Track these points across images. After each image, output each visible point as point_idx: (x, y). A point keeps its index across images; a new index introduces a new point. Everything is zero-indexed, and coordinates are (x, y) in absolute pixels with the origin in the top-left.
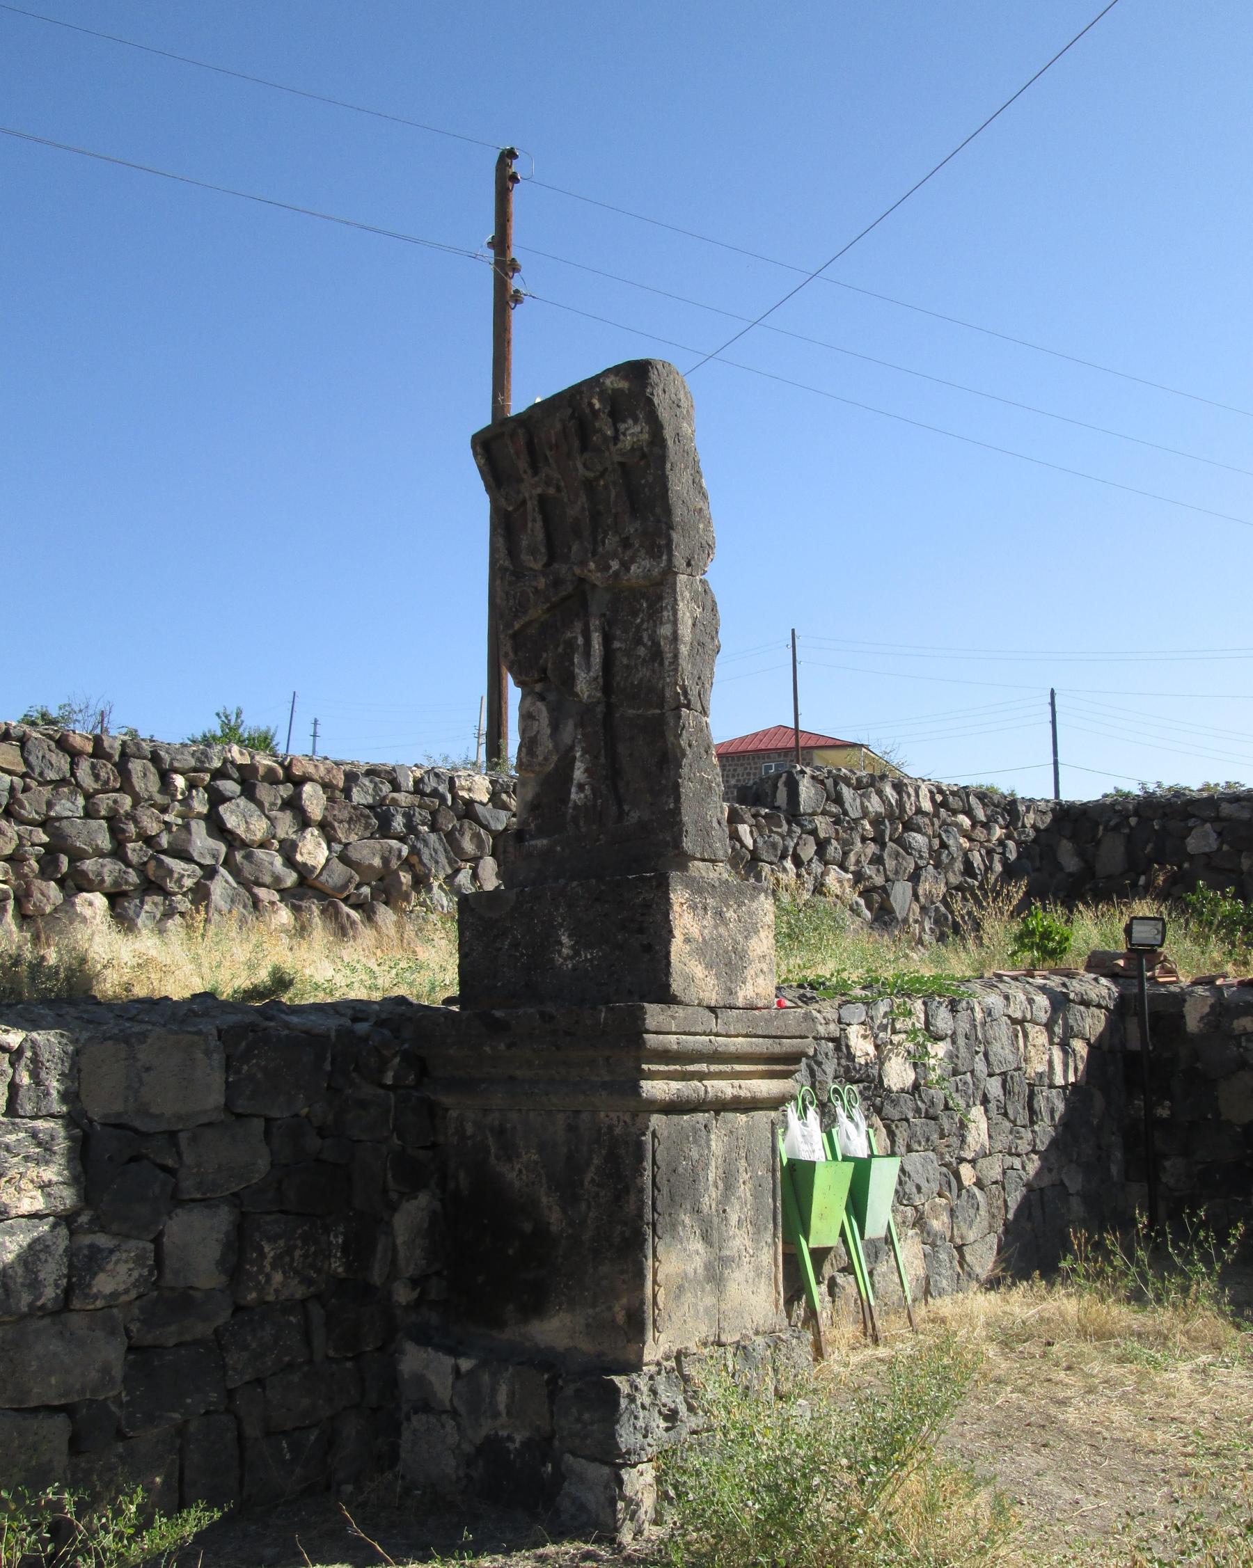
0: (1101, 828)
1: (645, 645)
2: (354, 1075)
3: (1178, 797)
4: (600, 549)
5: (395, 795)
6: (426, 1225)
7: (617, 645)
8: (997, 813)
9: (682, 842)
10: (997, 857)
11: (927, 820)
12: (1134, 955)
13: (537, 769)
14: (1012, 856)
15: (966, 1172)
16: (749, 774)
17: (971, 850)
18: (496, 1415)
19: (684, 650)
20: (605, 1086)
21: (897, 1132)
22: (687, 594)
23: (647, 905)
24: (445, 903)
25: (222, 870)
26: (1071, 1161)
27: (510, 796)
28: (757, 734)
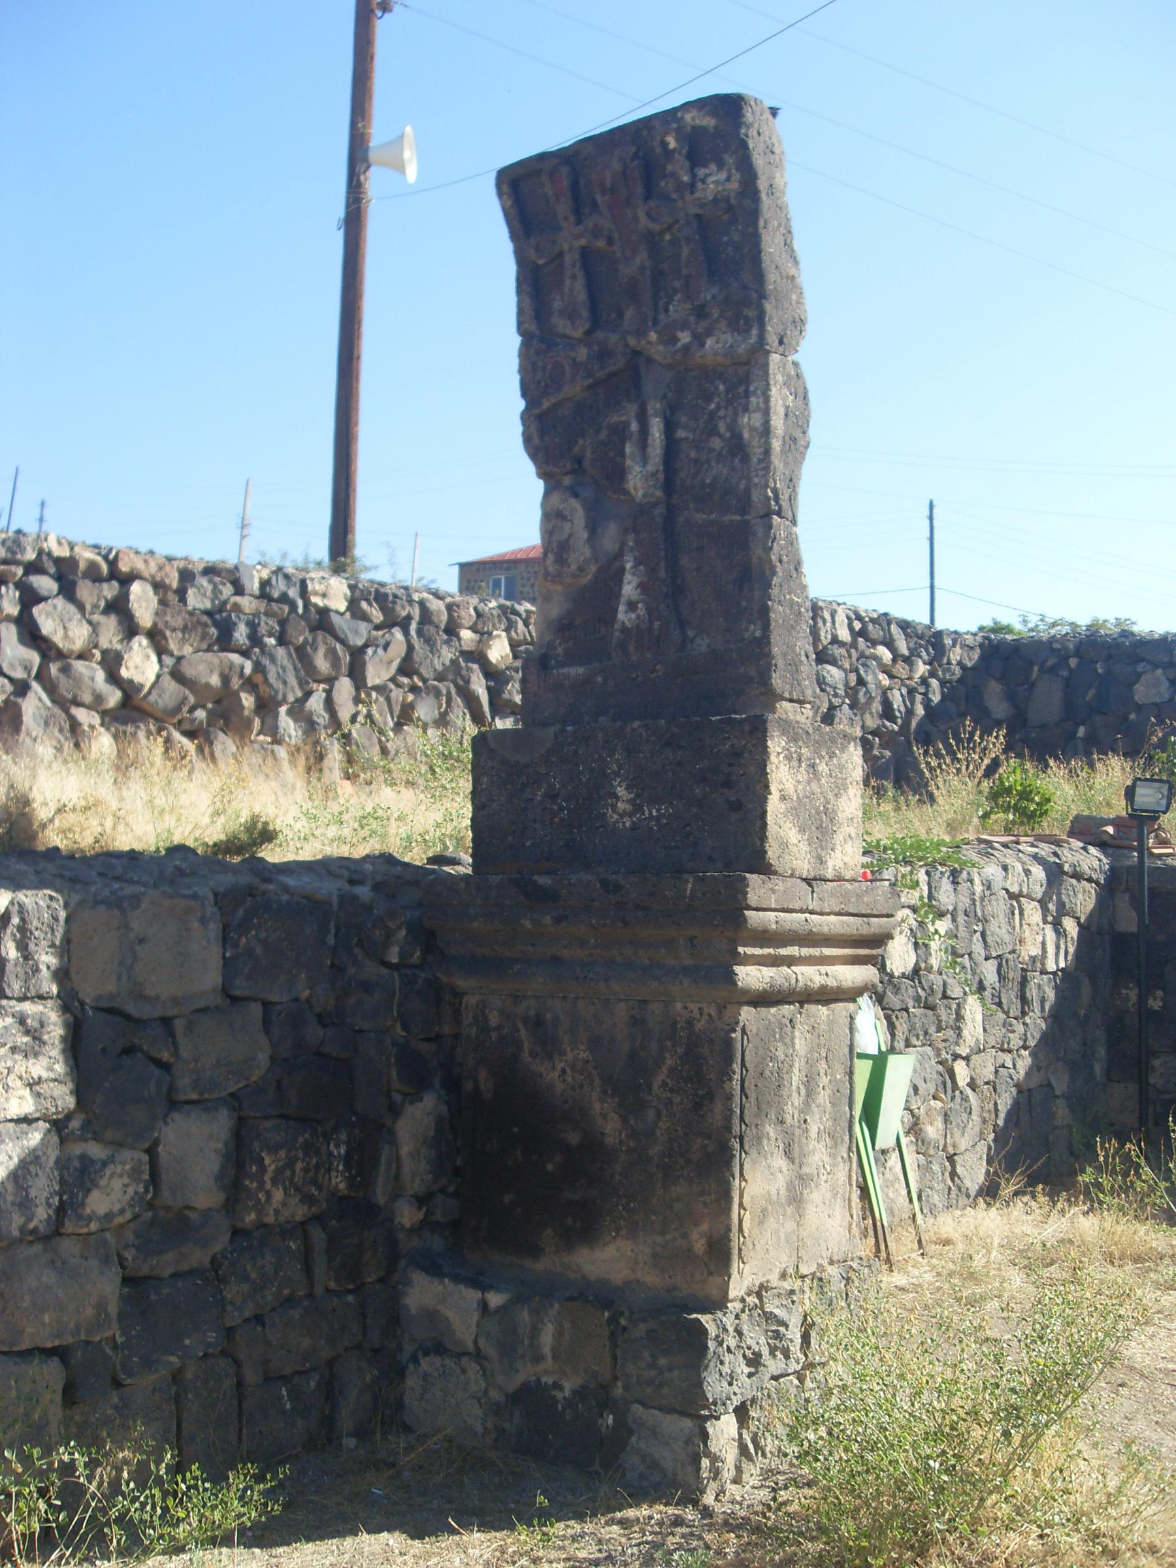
0: (1036, 668)
1: (720, 436)
2: (357, 951)
3: (1126, 637)
4: (662, 317)
5: (238, 599)
6: (432, 1133)
7: (681, 434)
8: (921, 646)
9: (770, 678)
10: (919, 698)
11: (843, 651)
12: (1135, 822)
13: (568, 580)
14: (936, 698)
15: (960, 1068)
17: (890, 688)
18: (538, 1358)
19: (776, 444)
20: (686, 971)
21: (897, 1023)
22: (780, 378)
23: (737, 754)
24: (293, 733)
25: (36, 686)
26: (1058, 1059)
27: (370, 605)
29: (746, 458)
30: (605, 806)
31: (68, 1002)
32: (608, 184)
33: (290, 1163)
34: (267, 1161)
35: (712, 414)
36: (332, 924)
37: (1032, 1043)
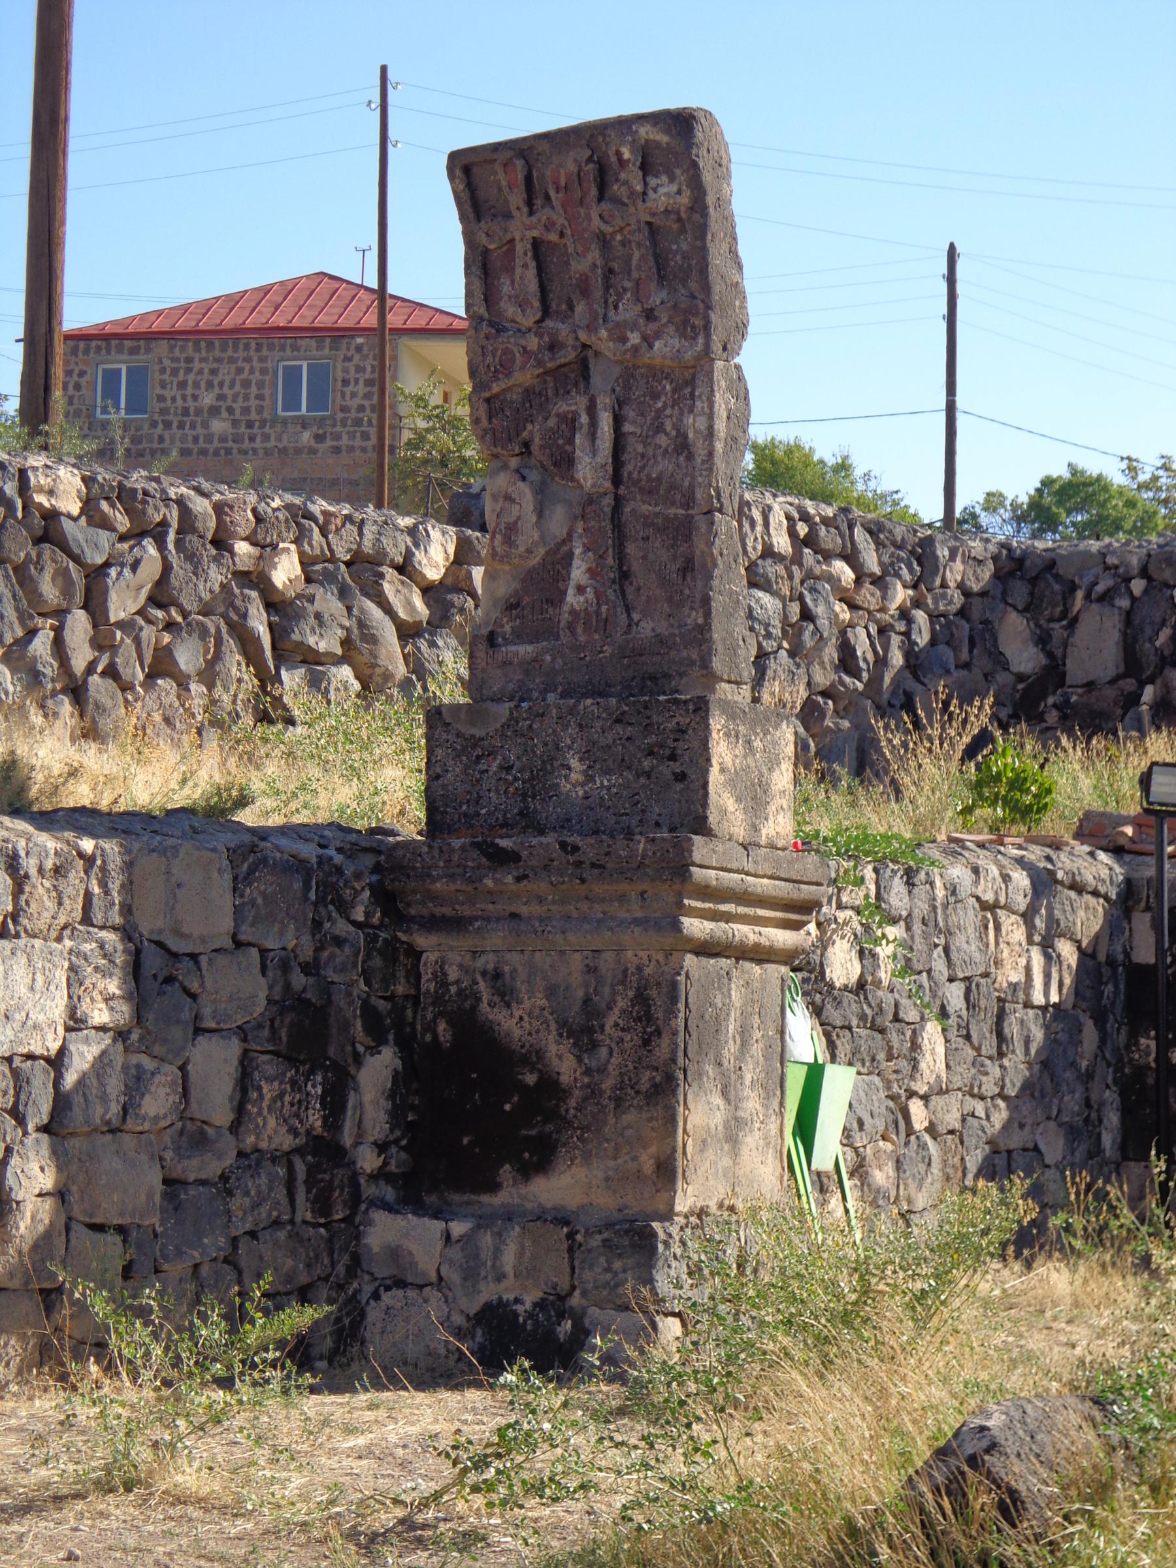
0: (1080, 594)
1: (667, 434)
2: (331, 907)
4: (611, 313)
8: (900, 560)
9: (711, 661)
10: (896, 640)
11: (780, 569)
12: (1152, 820)
13: (516, 561)
14: (922, 639)
15: (916, 1108)
16: (246, 384)
17: (851, 625)
18: (500, 1277)
19: (719, 447)
20: (636, 922)
21: (838, 1043)
22: (723, 383)
23: (681, 731)
24: (11, 688)
26: (1049, 1118)
27: (113, 506)
28: (266, 290)
29: (690, 457)
30: (559, 776)
31: (127, 932)
32: (563, 184)
33: (281, 1096)
34: (265, 1090)
35: (659, 412)
36: (314, 883)
37: (1012, 1092)
